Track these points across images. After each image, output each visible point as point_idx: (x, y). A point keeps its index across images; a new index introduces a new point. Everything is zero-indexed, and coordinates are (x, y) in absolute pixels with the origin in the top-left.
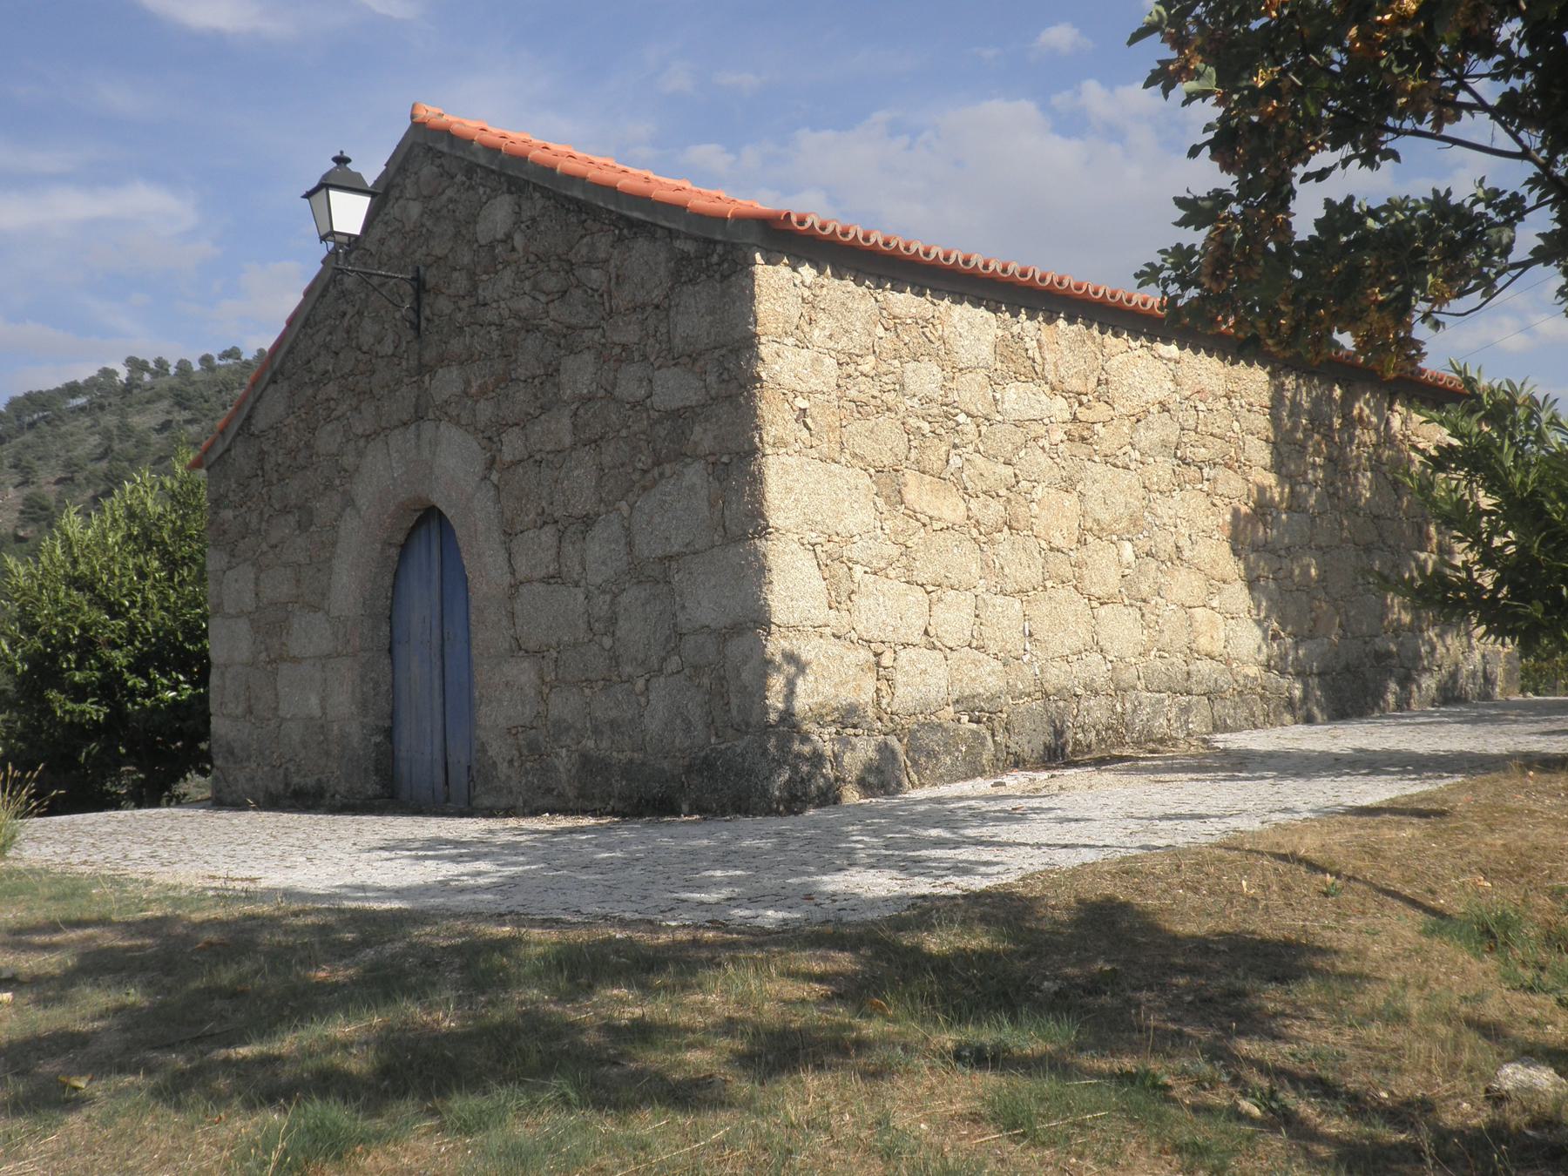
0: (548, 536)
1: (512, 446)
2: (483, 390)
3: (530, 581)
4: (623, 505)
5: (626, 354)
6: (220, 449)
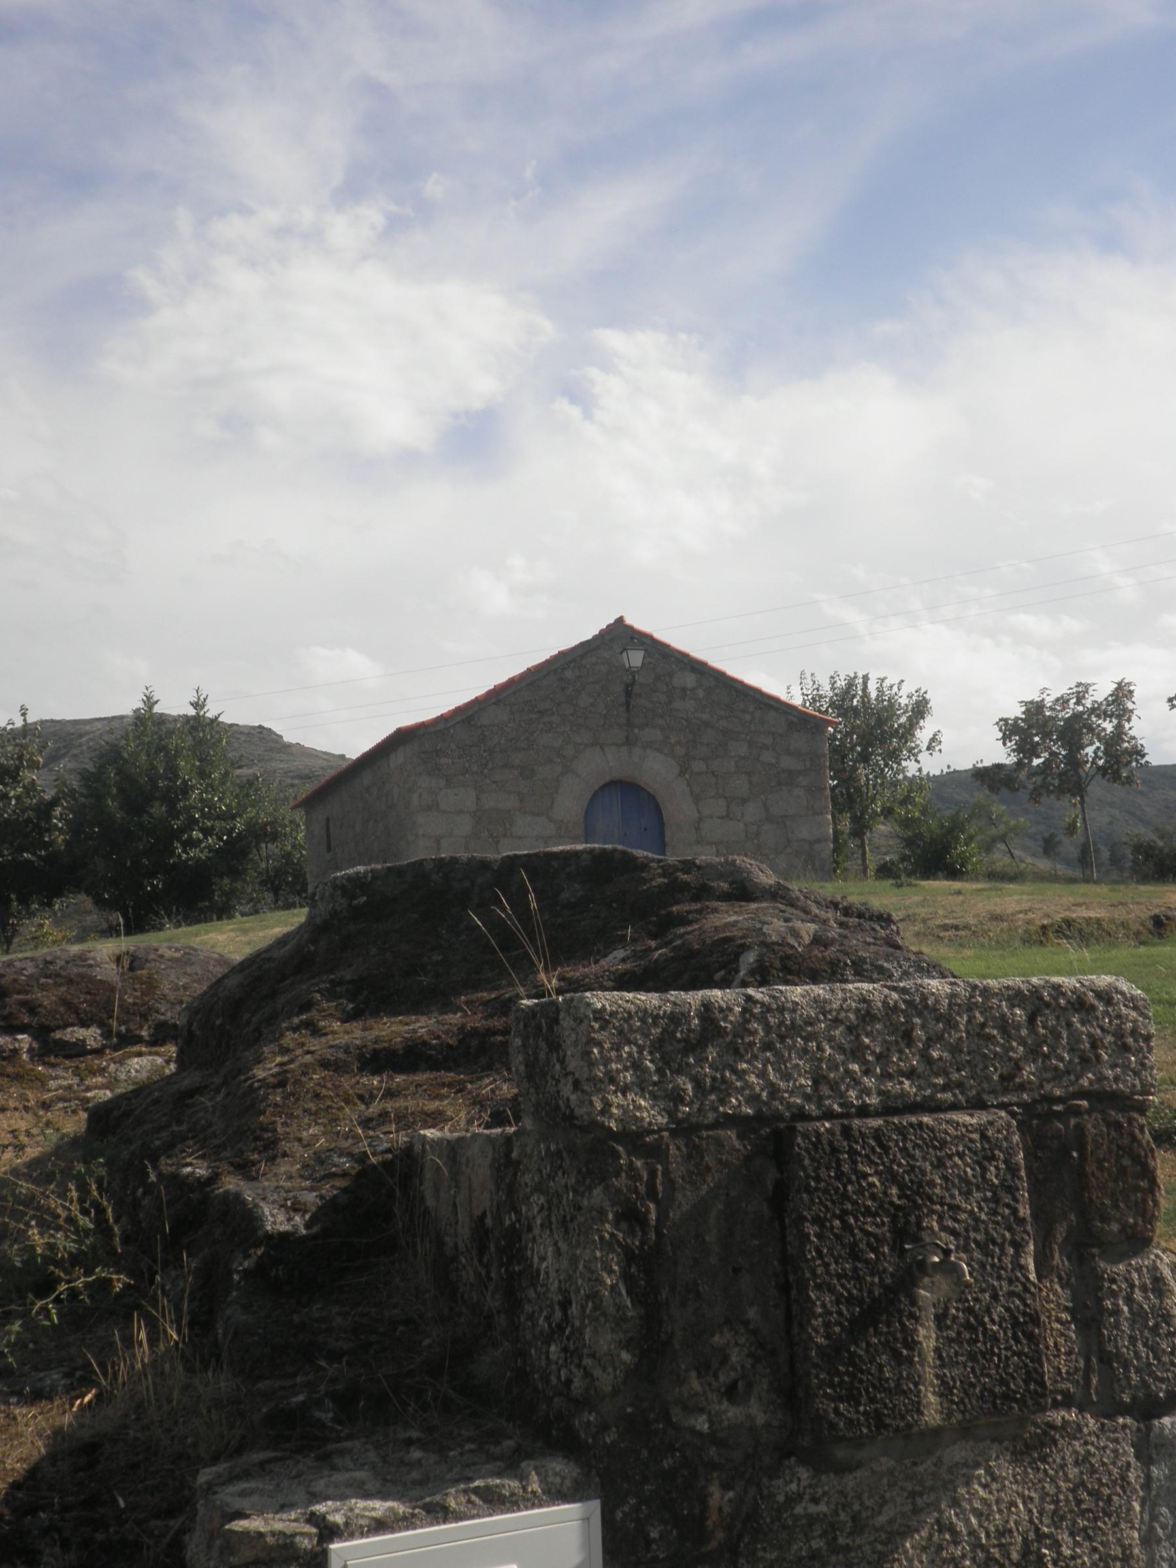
0: (722, 802)
1: (698, 766)
2: (679, 743)
3: (711, 817)
4: (762, 797)
5: (765, 747)
6: (441, 726)
